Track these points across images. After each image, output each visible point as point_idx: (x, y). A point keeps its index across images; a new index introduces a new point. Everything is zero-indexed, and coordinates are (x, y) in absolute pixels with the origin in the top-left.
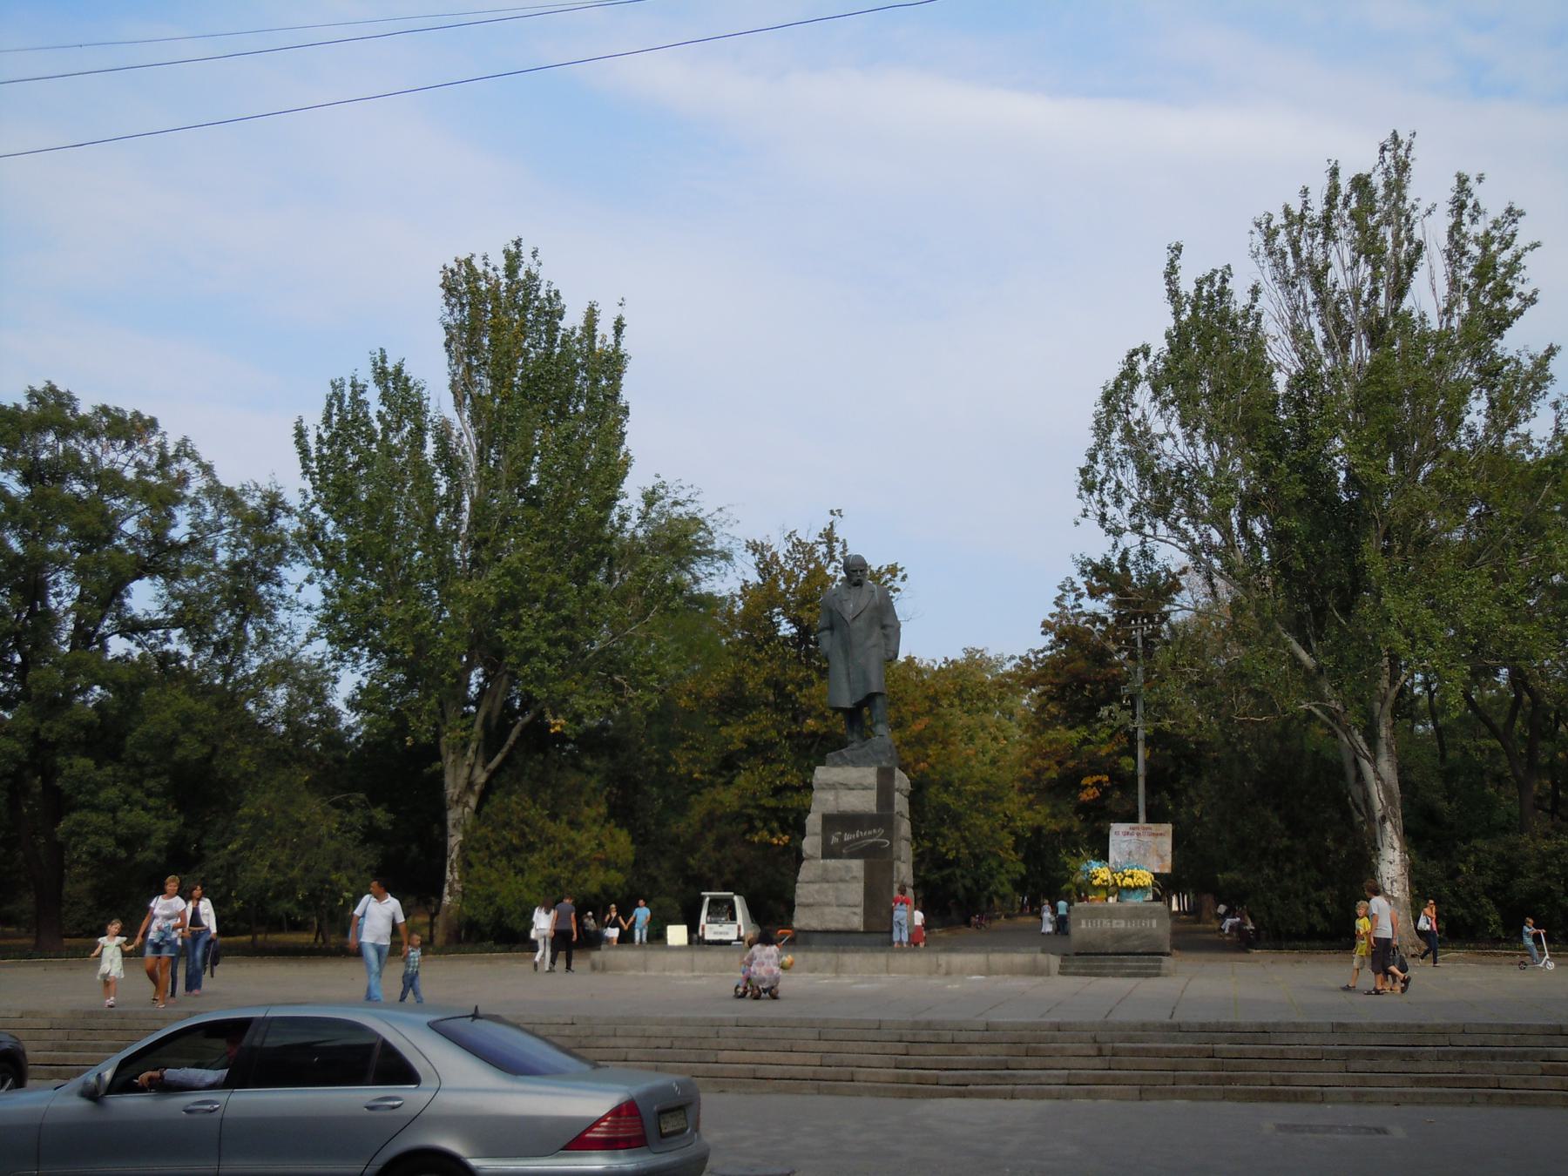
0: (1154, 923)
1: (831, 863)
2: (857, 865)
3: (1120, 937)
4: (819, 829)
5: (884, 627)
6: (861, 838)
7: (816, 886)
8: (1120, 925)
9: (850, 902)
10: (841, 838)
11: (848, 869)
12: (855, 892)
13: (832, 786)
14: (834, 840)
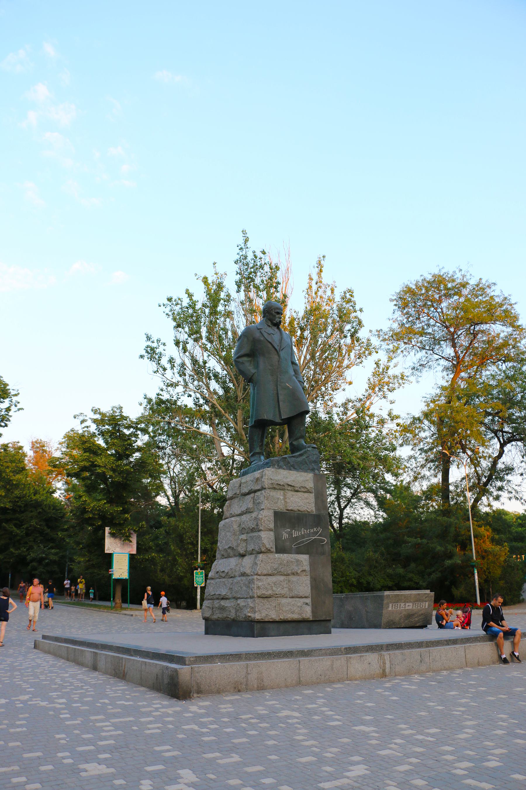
0: (427, 603)
1: (285, 557)
2: (304, 558)
4: (272, 526)
6: (303, 536)
9: (301, 594)
10: (290, 534)
14: (285, 536)
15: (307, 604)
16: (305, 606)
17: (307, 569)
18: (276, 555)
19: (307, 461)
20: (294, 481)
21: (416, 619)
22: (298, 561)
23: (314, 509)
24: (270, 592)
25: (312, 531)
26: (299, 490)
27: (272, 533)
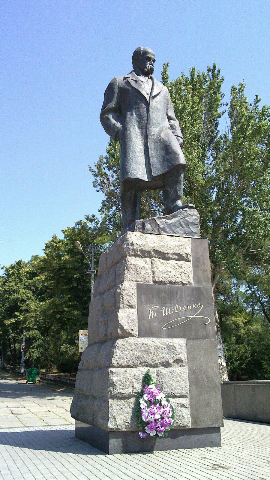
2: (180, 343)
4: (134, 301)
9: (176, 393)
11: (171, 348)
13: (145, 254)
15: (183, 406)
16: (180, 408)
17: (182, 358)
18: (139, 340)
19: (183, 223)
20: (163, 246)
22: (169, 346)
23: (192, 281)
26: (171, 256)
27: (134, 311)
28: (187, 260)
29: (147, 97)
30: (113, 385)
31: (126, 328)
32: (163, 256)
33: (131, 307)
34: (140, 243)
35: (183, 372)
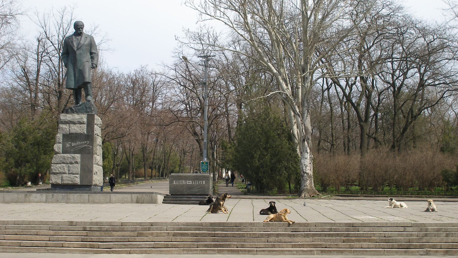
0: (204, 182)
2: (78, 156)
3: (190, 187)
5: (91, 53)
6: (78, 145)
7: (60, 165)
8: (190, 183)
10: (71, 145)
11: (74, 158)
12: (77, 168)
13: (66, 123)
14: (68, 145)
15: (76, 177)
21: (196, 190)
22: (73, 157)
23: (85, 132)
24: (57, 171)
25: (83, 143)
28: (84, 124)
29: (75, 49)
30: (52, 170)
31: (57, 150)
32: (74, 123)
33: (60, 143)
34: (64, 118)
35: (79, 166)
